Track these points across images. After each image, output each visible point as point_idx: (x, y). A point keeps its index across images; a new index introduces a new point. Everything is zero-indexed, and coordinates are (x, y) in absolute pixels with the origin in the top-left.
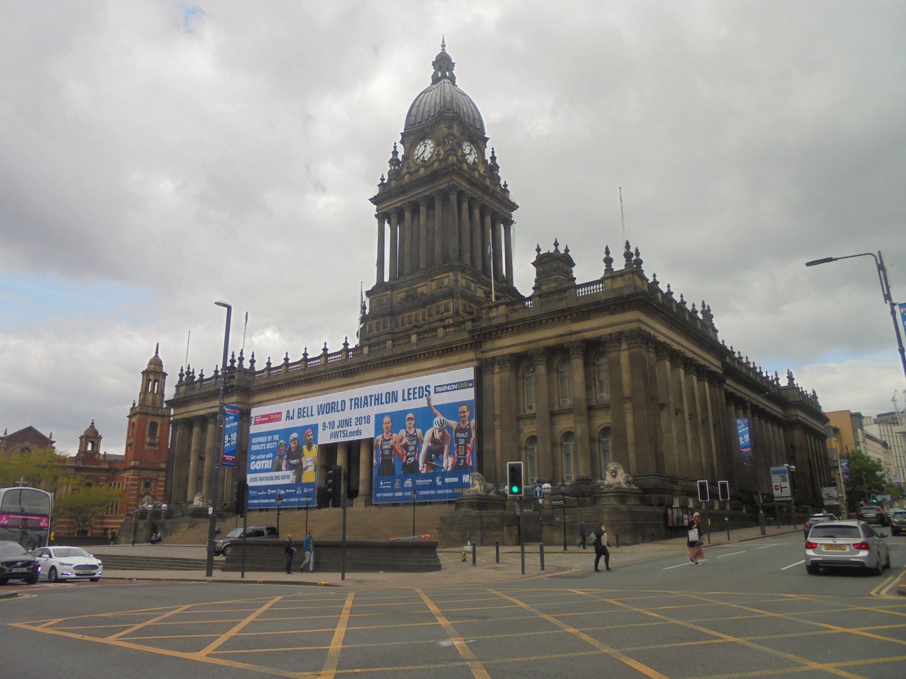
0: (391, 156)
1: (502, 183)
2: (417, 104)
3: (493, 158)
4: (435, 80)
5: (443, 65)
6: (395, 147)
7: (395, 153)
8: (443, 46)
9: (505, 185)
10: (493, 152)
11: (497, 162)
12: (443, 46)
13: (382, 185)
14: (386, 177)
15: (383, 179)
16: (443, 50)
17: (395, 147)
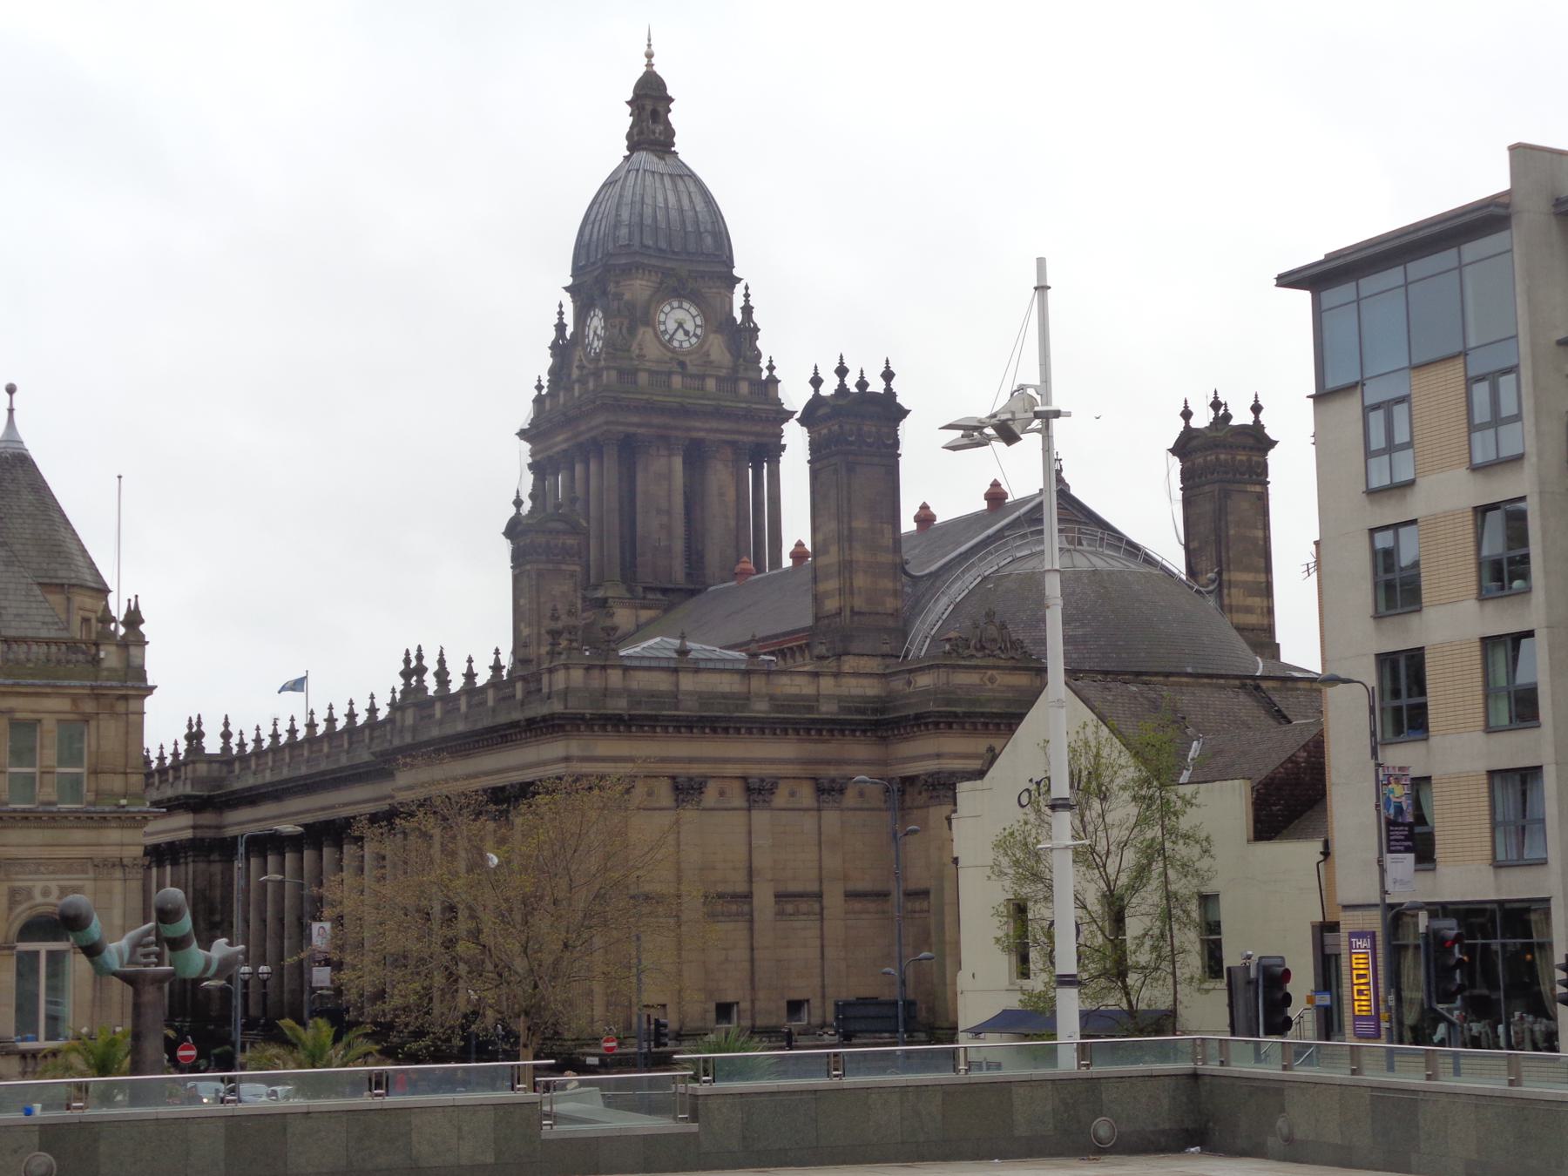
0: (552, 335)
1: (764, 363)
2: (592, 217)
3: (747, 310)
4: (634, 145)
5: (650, 101)
6: (561, 313)
7: (560, 327)
8: (649, 56)
9: (771, 368)
10: (747, 296)
11: (755, 317)
12: (649, 56)
13: (539, 401)
14: (545, 383)
15: (539, 387)
16: (650, 65)
17: (561, 313)
